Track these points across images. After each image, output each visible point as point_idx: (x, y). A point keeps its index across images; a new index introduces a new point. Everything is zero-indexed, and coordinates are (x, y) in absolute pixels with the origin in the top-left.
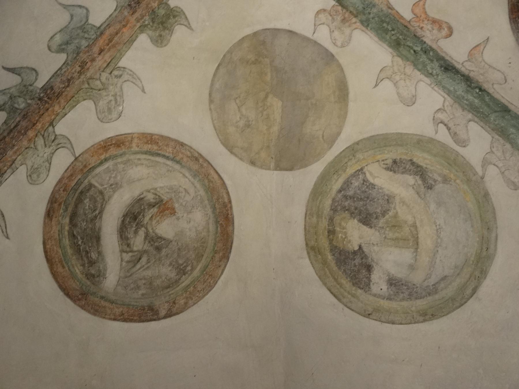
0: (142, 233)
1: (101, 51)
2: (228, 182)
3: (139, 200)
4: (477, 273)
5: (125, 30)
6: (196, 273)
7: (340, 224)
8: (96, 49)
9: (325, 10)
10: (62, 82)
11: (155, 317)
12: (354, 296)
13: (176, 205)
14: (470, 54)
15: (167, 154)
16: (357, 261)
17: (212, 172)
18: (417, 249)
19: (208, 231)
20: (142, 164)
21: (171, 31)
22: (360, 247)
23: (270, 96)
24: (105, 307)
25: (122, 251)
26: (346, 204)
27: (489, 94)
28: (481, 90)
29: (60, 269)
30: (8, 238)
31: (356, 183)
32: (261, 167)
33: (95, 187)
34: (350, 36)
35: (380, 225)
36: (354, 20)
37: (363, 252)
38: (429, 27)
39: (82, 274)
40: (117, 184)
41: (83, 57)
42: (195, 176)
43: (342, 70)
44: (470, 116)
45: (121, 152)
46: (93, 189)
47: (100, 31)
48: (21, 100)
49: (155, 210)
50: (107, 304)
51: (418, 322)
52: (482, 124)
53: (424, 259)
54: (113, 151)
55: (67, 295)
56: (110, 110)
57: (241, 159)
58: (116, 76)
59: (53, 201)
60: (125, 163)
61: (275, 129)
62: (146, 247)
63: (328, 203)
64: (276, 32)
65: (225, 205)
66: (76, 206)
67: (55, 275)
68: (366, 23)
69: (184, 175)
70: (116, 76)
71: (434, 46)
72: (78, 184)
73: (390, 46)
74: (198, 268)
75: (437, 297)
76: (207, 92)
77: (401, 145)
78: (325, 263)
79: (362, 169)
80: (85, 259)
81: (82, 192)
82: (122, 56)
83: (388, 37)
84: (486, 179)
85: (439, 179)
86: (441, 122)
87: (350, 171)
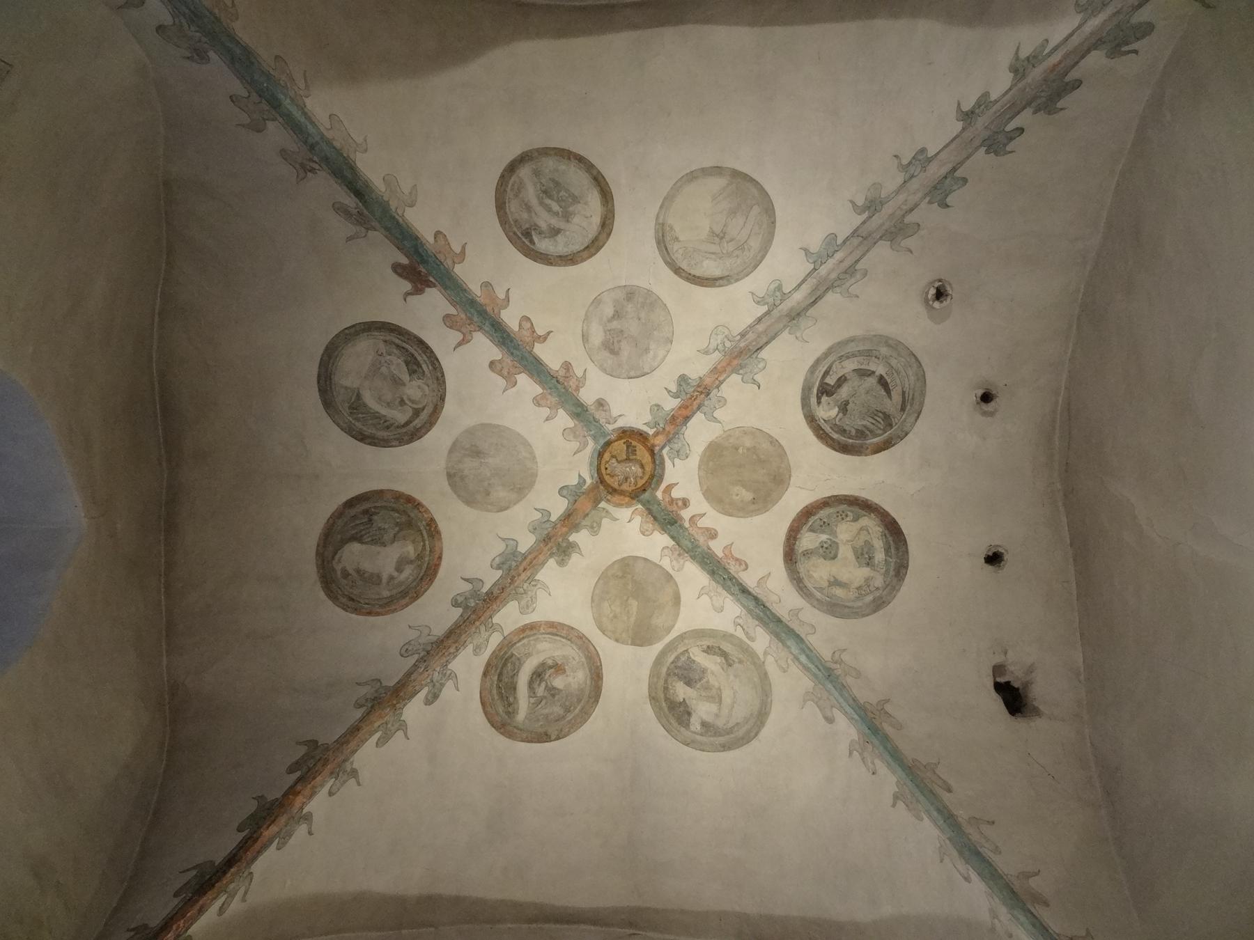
0: (543, 685)
1: (525, 570)
2: (600, 653)
3: (543, 664)
4: (759, 723)
5: (540, 556)
6: (577, 711)
7: (671, 683)
8: (521, 568)
9: (668, 547)
10: (499, 589)
11: (548, 740)
12: (678, 731)
13: (566, 667)
14: (758, 582)
15: (562, 635)
16: (682, 709)
17: (591, 647)
18: (720, 704)
19: (586, 684)
20: (546, 641)
21: (569, 556)
22: (684, 699)
23: (630, 598)
24: (516, 733)
25: (530, 697)
26: (676, 671)
27: (769, 609)
28: (764, 606)
29: (489, 709)
30: (458, 690)
31: (683, 659)
32: (623, 643)
33: (516, 656)
34: (683, 565)
35: (698, 687)
36: (686, 555)
37: (686, 703)
38: (734, 563)
39: (503, 711)
40: (529, 653)
41: (513, 573)
42: (579, 649)
43: (677, 586)
44: (757, 623)
45: (532, 633)
46: (514, 657)
47: (525, 557)
48: (472, 600)
49: (552, 670)
50: (519, 732)
51: (719, 751)
52: (764, 628)
53: (725, 711)
54: (528, 632)
55: (493, 725)
56: (528, 607)
57: (610, 638)
58: (533, 586)
59: (488, 665)
60: (535, 640)
61: (633, 619)
62: (545, 694)
63: (664, 670)
64: (636, 558)
65: (597, 667)
66: (502, 668)
67: (486, 713)
68: (693, 558)
69: (573, 648)
70: (533, 586)
71: (736, 576)
72: (506, 653)
73: (708, 574)
74: (579, 708)
75: (732, 736)
76: (591, 594)
77: (713, 637)
78: (661, 708)
79: (687, 650)
80: (506, 703)
81: (506, 659)
82: (537, 573)
83: (707, 568)
84: (766, 664)
85: (736, 660)
86: (739, 625)
87: (680, 650)
